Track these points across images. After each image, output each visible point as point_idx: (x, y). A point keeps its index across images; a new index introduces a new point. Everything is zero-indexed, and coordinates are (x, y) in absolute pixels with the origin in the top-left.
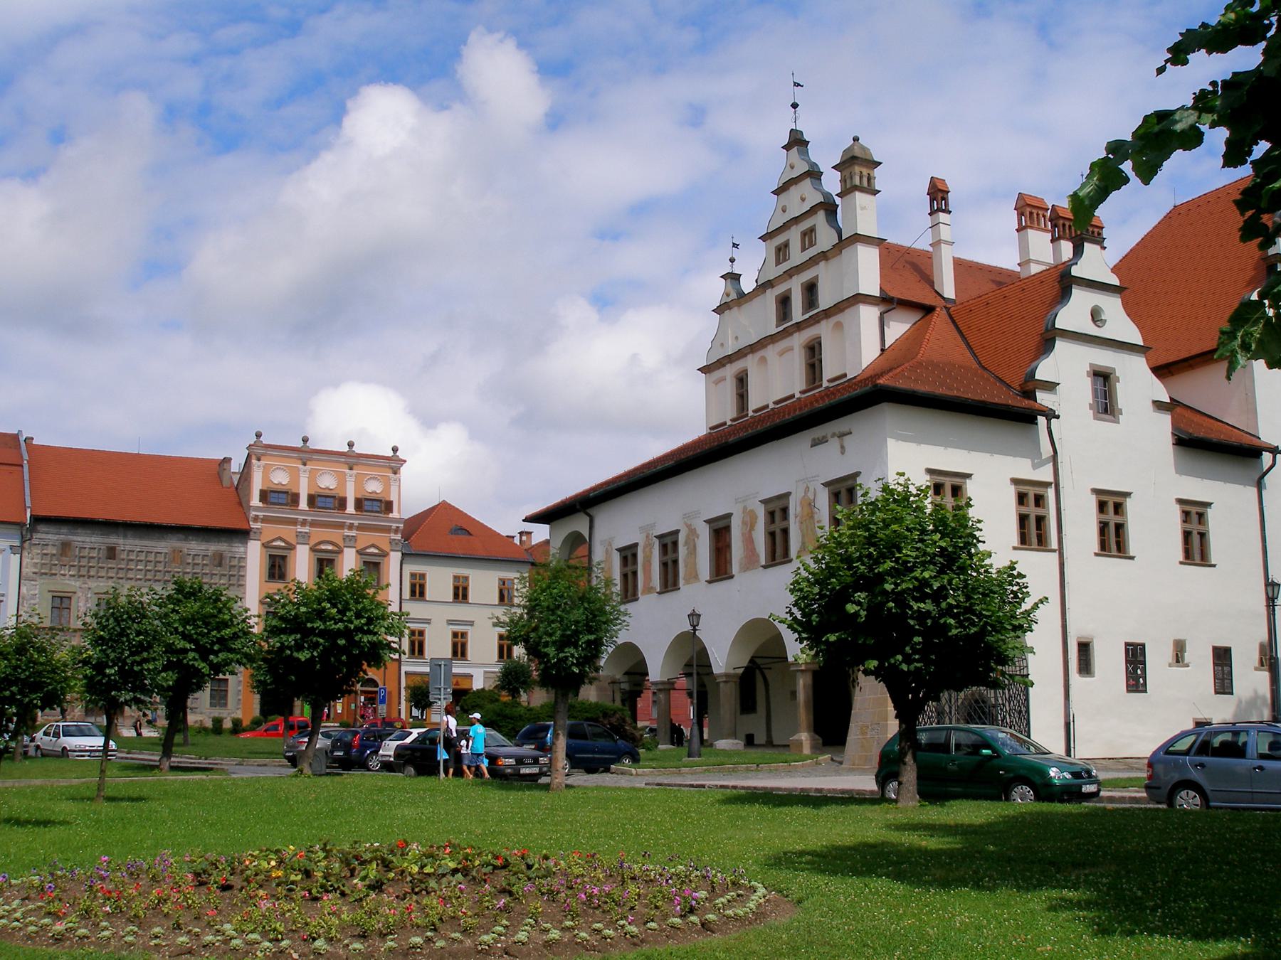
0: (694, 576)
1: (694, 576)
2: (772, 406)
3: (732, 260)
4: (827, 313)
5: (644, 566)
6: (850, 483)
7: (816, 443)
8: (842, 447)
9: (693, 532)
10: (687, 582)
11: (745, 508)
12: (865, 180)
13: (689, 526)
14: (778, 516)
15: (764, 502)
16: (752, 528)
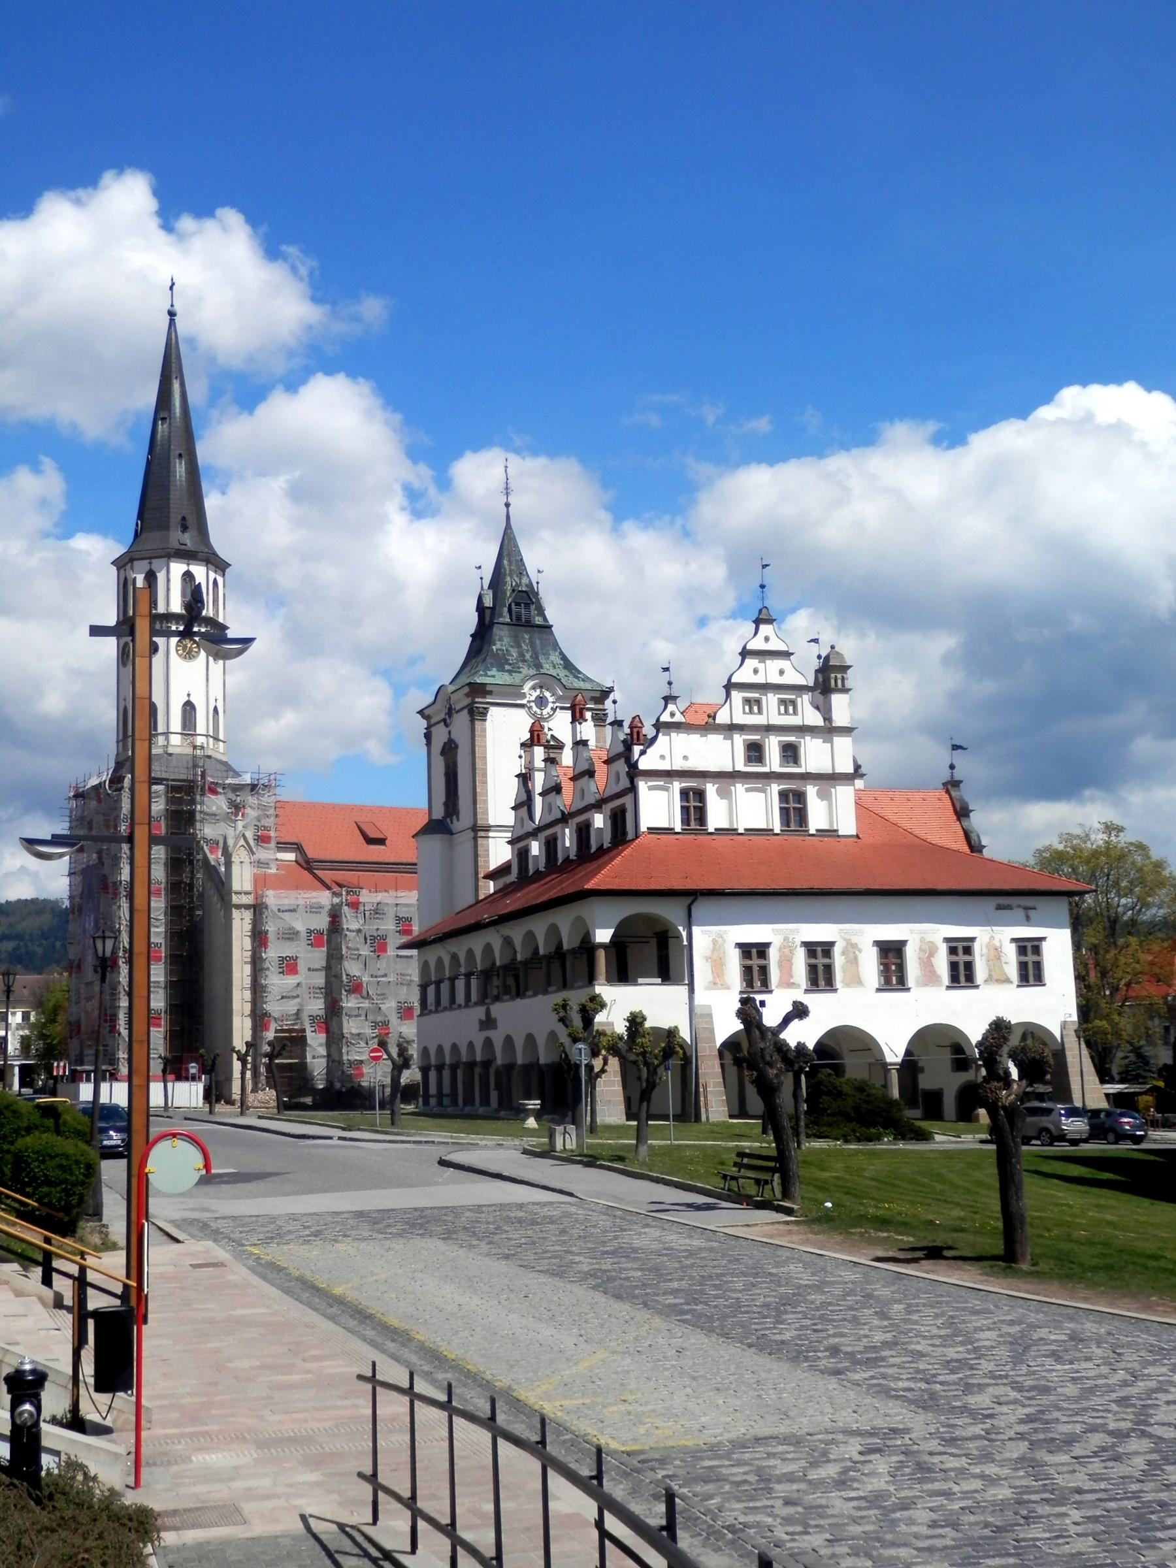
0: (856, 980)
1: (856, 980)
2: (741, 831)
3: (670, 683)
5: (780, 965)
6: (1036, 943)
7: (999, 907)
10: (848, 984)
11: (922, 940)
12: (839, 682)
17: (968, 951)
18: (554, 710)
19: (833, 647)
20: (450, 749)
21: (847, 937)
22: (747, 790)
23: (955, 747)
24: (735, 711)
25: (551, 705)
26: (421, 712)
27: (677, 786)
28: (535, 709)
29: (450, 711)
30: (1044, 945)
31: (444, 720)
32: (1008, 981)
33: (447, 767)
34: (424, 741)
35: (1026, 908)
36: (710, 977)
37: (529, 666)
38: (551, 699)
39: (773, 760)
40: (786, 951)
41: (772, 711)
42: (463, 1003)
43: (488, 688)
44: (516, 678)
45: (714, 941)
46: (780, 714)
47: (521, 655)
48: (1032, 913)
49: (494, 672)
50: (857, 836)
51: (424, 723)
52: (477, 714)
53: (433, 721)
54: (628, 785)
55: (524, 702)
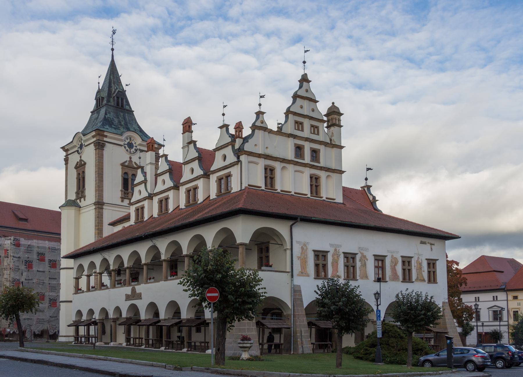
1: (365, 276)
2: (293, 193)
4: (328, 170)
5: (332, 263)
7: (422, 243)
8: (431, 248)
9: (364, 258)
10: (362, 278)
11: (392, 256)
13: (362, 254)
14: (407, 264)
15: (402, 257)
16: (396, 264)
17: (409, 262)
18: (136, 150)
19: (333, 103)
20: (81, 166)
21: (362, 252)
22: (296, 171)
23: (368, 169)
24: (289, 129)
25: (134, 148)
26: (63, 148)
27: (262, 163)
28: (127, 148)
29: (81, 147)
30: (438, 263)
31: (77, 151)
32: (424, 280)
33: (79, 174)
34: (64, 162)
35: (431, 244)
36: (299, 269)
37: (124, 128)
38: (135, 145)
39: (307, 159)
40: (336, 256)
41: (306, 133)
42: (85, 290)
43: (105, 134)
44: (119, 132)
45: (302, 248)
46: (311, 133)
47: (120, 122)
48: (433, 246)
49: (107, 127)
50: (343, 203)
51: (64, 154)
52: (100, 146)
53: (69, 152)
54: (235, 159)
55: (122, 143)
